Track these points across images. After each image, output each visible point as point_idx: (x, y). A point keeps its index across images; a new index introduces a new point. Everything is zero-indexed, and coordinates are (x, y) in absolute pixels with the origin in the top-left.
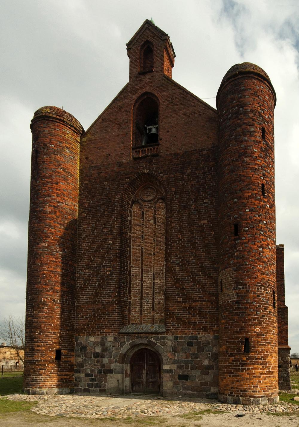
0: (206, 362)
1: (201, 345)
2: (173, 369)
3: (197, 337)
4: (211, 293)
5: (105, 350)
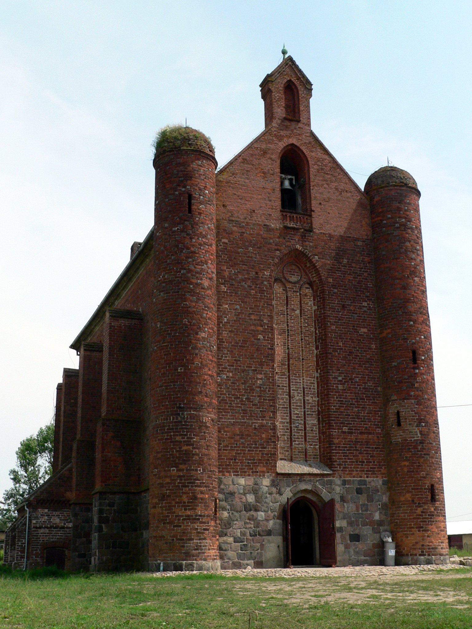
0: (377, 516)
1: (371, 493)
2: (343, 526)
3: (365, 481)
4: (376, 423)
5: (258, 499)
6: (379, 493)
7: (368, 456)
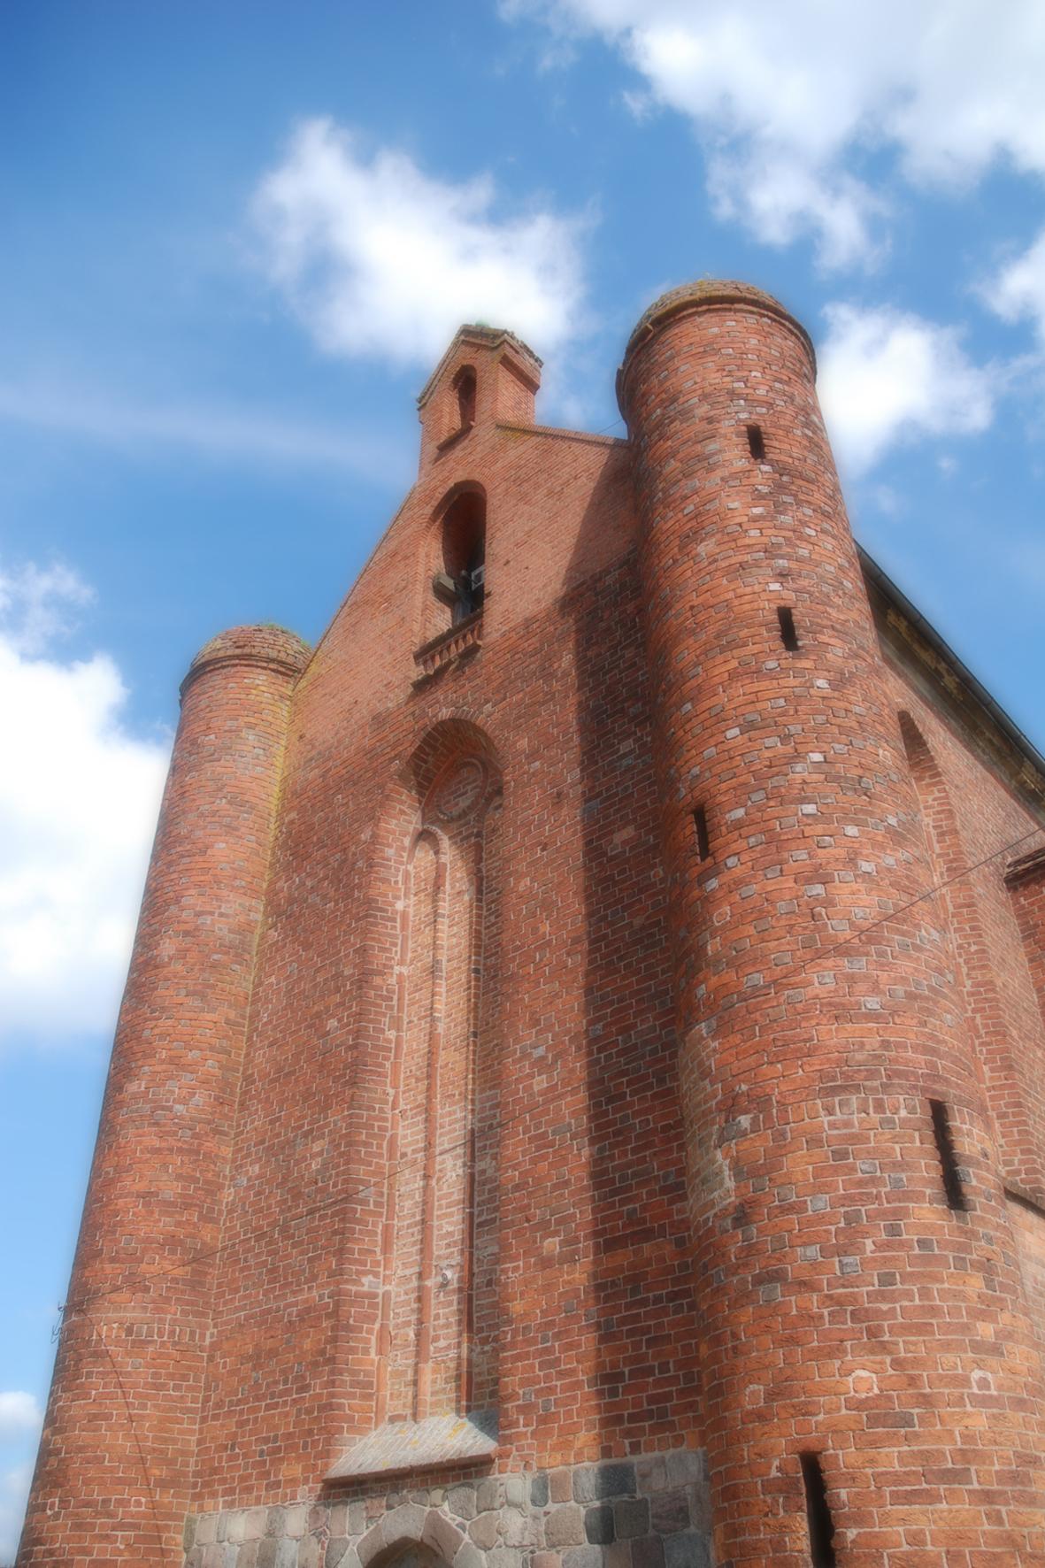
1: (651, 1533)
6: (692, 1529)
7: (636, 1346)
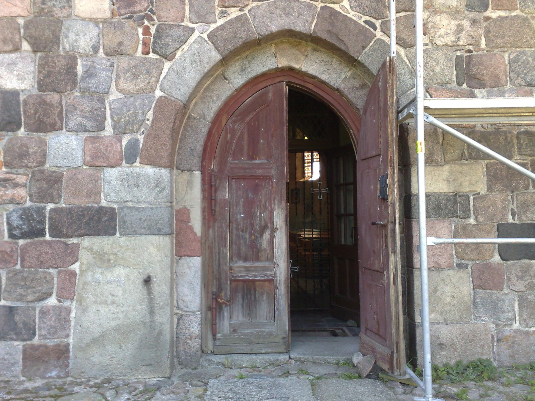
2: (466, 189)
